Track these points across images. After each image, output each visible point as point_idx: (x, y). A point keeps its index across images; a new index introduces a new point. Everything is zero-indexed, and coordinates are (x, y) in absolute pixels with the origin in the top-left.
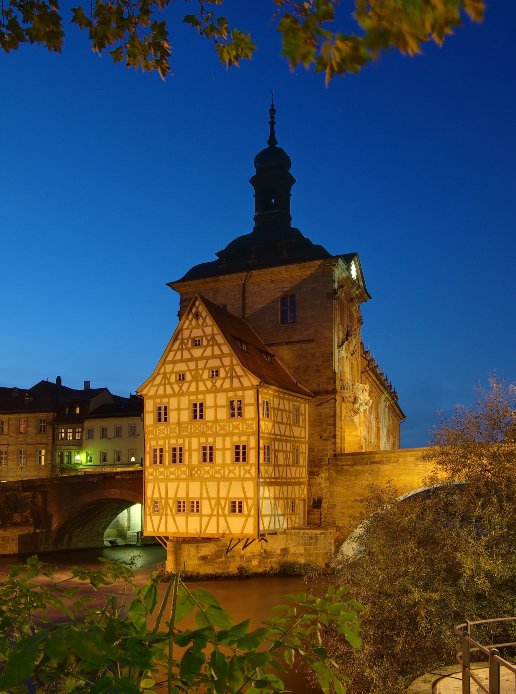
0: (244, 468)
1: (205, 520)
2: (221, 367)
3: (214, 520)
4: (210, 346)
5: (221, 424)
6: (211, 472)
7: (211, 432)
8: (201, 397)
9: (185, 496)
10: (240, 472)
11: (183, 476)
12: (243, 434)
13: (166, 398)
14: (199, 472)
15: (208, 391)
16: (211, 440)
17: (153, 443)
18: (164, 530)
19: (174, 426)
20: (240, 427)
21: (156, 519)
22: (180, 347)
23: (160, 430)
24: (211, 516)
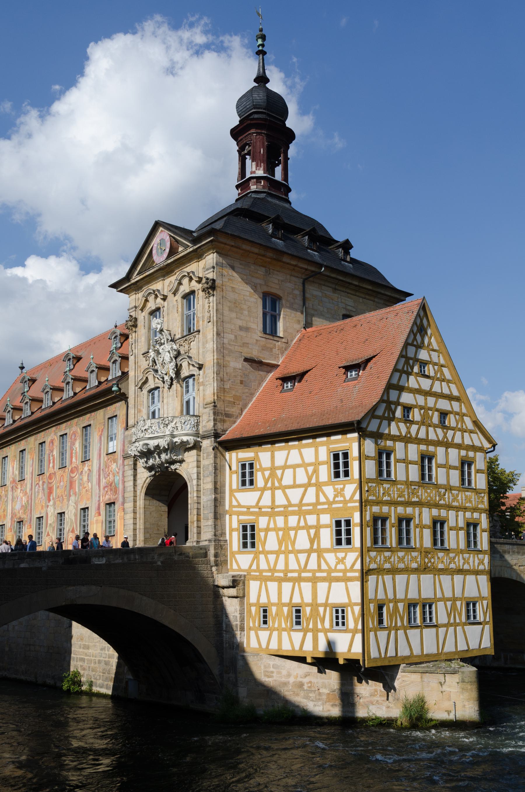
0: (477, 557)
1: (442, 630)
2: (451, 412)
3: (451, 629)
4: (438, 379)
5: (453, 492)
6: (445, 561)
7: (444, 502)
8: (431, 448)
9: (417, 597)
10: (474, 562)
11: (414, 565)
12: (475, 510)
13: (390, 440)
14: (432, 560)
15: (438, 443)
16: (443, 513)
17: (376, 509)
18: (394, 655)
19: (403, 487)
20: (473, 499)
21: (382, 635)
22: (405, 369)
23: (384, 489)
24: (447, 625)
